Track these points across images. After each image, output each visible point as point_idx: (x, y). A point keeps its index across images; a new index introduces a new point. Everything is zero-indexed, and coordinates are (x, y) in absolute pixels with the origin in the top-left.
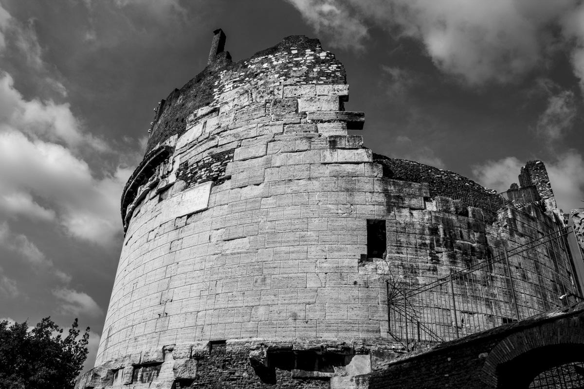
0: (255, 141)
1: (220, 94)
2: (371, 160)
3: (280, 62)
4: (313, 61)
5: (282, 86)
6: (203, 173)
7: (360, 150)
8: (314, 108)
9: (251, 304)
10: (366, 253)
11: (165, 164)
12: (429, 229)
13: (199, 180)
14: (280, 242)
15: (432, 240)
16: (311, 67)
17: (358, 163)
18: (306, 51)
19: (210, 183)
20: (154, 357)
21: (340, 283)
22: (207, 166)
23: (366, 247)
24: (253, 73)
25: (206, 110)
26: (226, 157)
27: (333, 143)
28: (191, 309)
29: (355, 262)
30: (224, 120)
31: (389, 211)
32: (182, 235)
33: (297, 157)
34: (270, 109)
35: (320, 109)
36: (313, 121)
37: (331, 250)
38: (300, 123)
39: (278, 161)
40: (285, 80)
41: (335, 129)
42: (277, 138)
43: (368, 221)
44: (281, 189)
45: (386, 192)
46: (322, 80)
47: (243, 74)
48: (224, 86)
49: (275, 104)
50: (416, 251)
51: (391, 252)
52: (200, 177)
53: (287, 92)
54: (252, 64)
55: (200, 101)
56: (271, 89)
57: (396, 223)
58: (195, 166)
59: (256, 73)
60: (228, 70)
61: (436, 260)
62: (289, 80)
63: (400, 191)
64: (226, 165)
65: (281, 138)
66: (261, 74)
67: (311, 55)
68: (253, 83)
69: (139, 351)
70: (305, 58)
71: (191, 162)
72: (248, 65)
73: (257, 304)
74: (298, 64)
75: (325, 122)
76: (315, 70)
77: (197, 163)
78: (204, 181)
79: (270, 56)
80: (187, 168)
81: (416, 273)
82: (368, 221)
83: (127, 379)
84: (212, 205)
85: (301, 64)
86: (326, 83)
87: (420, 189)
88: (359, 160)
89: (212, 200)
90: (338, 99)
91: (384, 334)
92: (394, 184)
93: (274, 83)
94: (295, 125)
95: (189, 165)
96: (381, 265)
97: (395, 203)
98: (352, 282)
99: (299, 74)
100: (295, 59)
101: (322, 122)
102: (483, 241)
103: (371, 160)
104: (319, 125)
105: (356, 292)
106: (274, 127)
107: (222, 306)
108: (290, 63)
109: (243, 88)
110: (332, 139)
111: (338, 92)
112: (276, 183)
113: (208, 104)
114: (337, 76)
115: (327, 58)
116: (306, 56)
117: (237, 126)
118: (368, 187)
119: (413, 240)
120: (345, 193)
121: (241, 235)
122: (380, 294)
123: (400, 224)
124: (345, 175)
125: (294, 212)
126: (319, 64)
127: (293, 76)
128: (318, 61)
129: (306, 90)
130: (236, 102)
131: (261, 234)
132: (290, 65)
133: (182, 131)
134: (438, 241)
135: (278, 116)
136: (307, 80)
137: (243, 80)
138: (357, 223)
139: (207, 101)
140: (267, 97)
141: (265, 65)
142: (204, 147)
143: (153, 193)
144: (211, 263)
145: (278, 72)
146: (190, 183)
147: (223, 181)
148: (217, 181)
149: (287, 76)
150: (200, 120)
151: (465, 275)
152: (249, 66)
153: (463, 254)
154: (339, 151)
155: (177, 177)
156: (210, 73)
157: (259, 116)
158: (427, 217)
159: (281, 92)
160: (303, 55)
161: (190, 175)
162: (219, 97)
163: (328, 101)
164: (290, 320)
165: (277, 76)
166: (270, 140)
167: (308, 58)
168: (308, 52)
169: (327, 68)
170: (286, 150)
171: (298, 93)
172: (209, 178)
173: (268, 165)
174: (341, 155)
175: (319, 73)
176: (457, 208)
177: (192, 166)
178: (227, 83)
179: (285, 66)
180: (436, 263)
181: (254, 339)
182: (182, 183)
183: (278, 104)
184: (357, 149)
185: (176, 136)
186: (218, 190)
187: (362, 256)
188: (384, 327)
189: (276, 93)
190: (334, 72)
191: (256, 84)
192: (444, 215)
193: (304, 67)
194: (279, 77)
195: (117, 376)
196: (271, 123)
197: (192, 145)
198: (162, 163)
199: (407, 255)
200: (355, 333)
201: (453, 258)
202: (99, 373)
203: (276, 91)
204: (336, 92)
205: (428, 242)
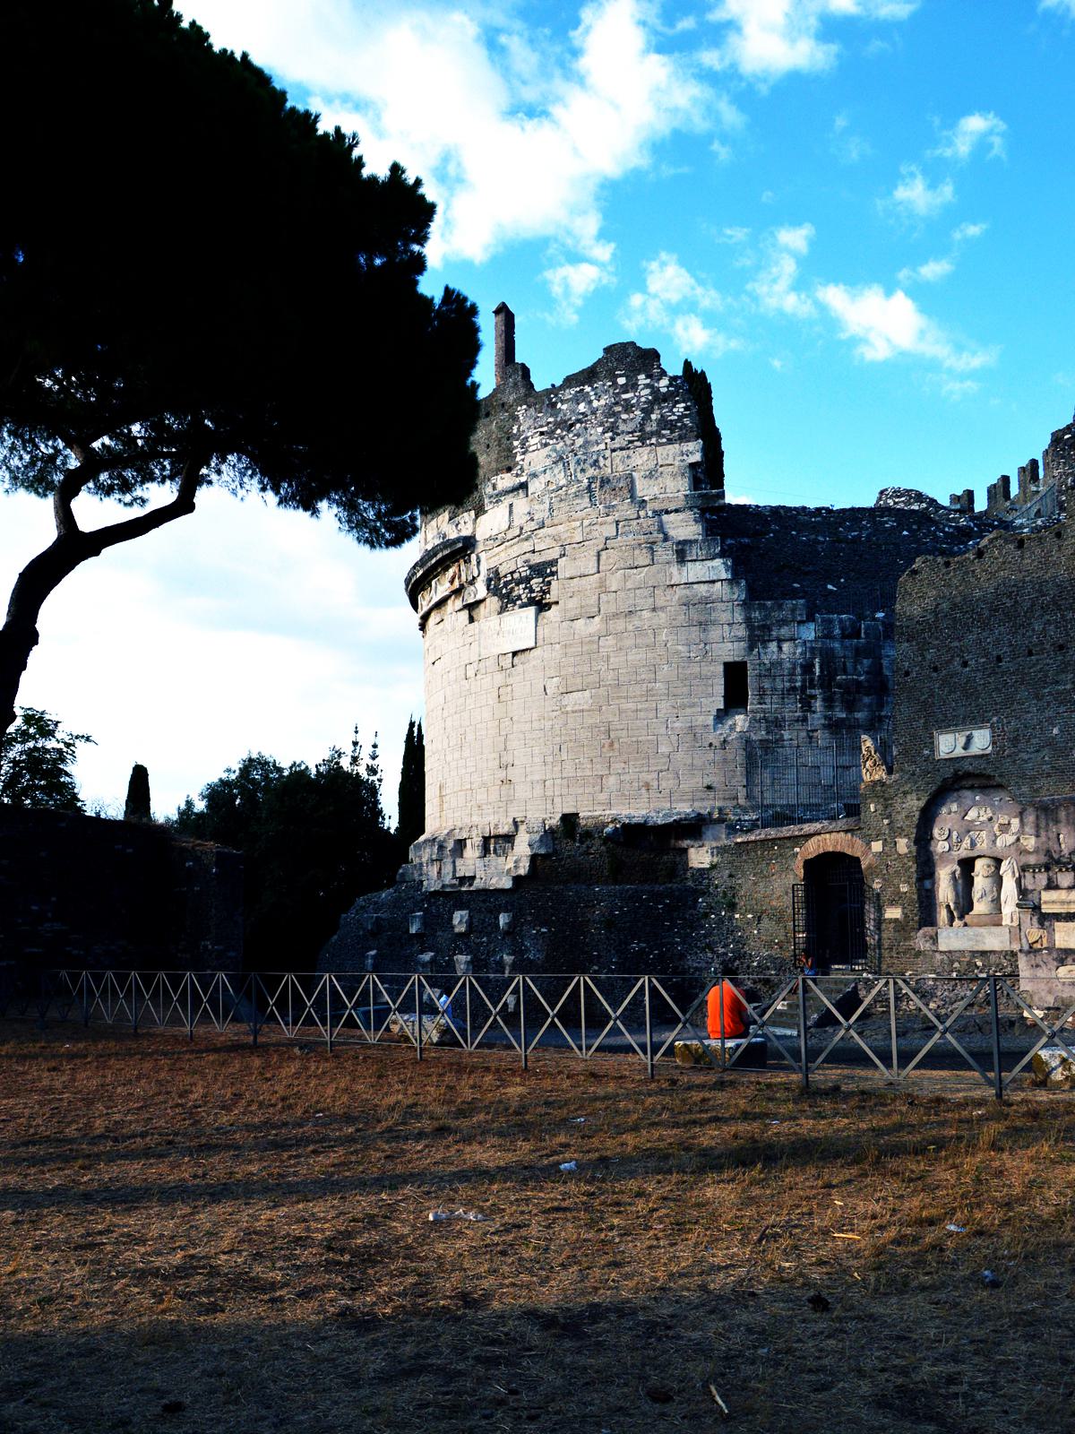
0: (582, 549)
1: (524, 453)
2: (730, 577)
3: (602, 402)
5: (609, 451)
6: (520, 590)
7: (717, 560)
8: (656, 488)
9: (601, 773)
10: (722, 707)
11: (465, 562)
12: (802, 666)
13: (519, 602)
14: (627, 697)
15: (804, 681)
16: (647, 412)
17: (713, 582)
18: (639, 377)
19: (532, 610)
20: (504, 830)
21: (694, 747)
22: (527, 580)
23: (722, 699)
24: (566, 422)
25: (505, 481)
26: (548, 571)
27: (682, 553)
28: (537, 777)
29: (710, 720)
30: (537, 507)
31: (751, 648)
32: (510, 681)
33: (639, 576)
34: (597, 494)
35: (663, 491)
36: (654, 512)
37: (683, 707)
38: (639, 517)
39: (614, 582)
40: (612, 439)
41: (685, 527)
43: (726, 665)
44: (620, 625)
45: (748, 621)
46: (664, 436)
47: (551, 420)
48: (527, 438)
49: (601, 487)
50: (783, 698)
51: (752, 704)
52: (519, 597)
53: (617, 461)
54: (563, 402)
55: (497, 460)
56: (595, 457)
57: (760, 665)
58: (509, 578)
60: (529, 406)
61: (807, 704)
62: (618, 439)
63: (766, 617)
66: (578, 425)
67: (647, 386)
68: (569, 442)
69: (486, 820)
71: (503, 571)
72: (556, 403)
73: (607, 772)
74: (628, 407)
75: (671, 512)
76: (653, 417)
77: (512, 573)
79: (587, 389)
80: (500, 579)
81: (781, 726)
83: (477, 853)
84: (540, 642)
85: (633, 406)
86: (670, 442)
87: (793, 610)
88: (715, 578)
89: (540, 637)
90: (688, 470)
91: (742, 801)
92: (762, 607)
93: (598, 444)
94: (631, 522)
95: (501, 575)
96: (740, 721)
97: (758, 636)
98: (706, 744)
100: (624, 396)
101: (667, 512)
102: (876, 670)
103: (730, 577)
104: (665, 518)
105: (711, 756)
106: (604, 527)
107: (570, 775)
108: (616, 404)
109: (555, 450)
110: (680, 547)
112: (616, 615)
113: (509, 470)
114: (686, 425)
116: (640, 387)
117: (556, 521)
118: (725, 617)
119: (780, 686)
121: (580, 688)
122: (737, 755)
123: (765, 664)
125: (638, 657)
126: (659, 404)
127: (623, 432)
128: (658, 398)
129: (642, 458)
130: (548, 476)
131: (604, 686)
132: (618, 409)
133: (480, 511)
134: (812, 680)
135: (608, 507)
136: (642, 439)
137: (553, 432)
138: (712, 669)
139: (507, 463)
140: (591, 472)
141: (582, 407)
142: (516, 550)
143: (459, 604)
144: (550, 723)
145: (601, 424)
146: (507, 603)
147: (548, 606)
148: (542, 606)
149: (613, 429)
150: (502, 498)
151: (843, 719)
152: (559, 405)
153: (842, 694)
154: (689, 564)
155: (488, 589)
156: (503, 405)
157: (582, 507)
158: (799, 650)
159: (608, 463)
161: (504, 591)
162: (523, 460)
163: (674, 475)
164: (643, 791)
165: (600, 430)
166: (601, 546)
167: (642, 393)
168: (642, 377)
169: (671, 411)
170: (622, 566)
172: (531, 602)
173: (603, 588)
174: (695, 571)
176: (842, 629)
177: (505, 576)
178: (529, 434)
179: (610, 412)
180: (807, 711)
181: (607, 812)
182: (493, 603)
183: (607, 487)
185: (473, 513)
186: (545, 621)
187: (718, 710)
188: (742, 793)
189: (601, 465)
190: (681, 418)
191: (573, 444)
192: (823, 643)
193: (638, 413)
194: (604, 433)
195: (465, 846)
196: (600, 520)
197: (498, 540)
198: (462, 561)
200: (711, 802)
201: (829, 702)
202: (445, 844)
203: (601, 459)
204: (685, 457)
205: (798, 684)
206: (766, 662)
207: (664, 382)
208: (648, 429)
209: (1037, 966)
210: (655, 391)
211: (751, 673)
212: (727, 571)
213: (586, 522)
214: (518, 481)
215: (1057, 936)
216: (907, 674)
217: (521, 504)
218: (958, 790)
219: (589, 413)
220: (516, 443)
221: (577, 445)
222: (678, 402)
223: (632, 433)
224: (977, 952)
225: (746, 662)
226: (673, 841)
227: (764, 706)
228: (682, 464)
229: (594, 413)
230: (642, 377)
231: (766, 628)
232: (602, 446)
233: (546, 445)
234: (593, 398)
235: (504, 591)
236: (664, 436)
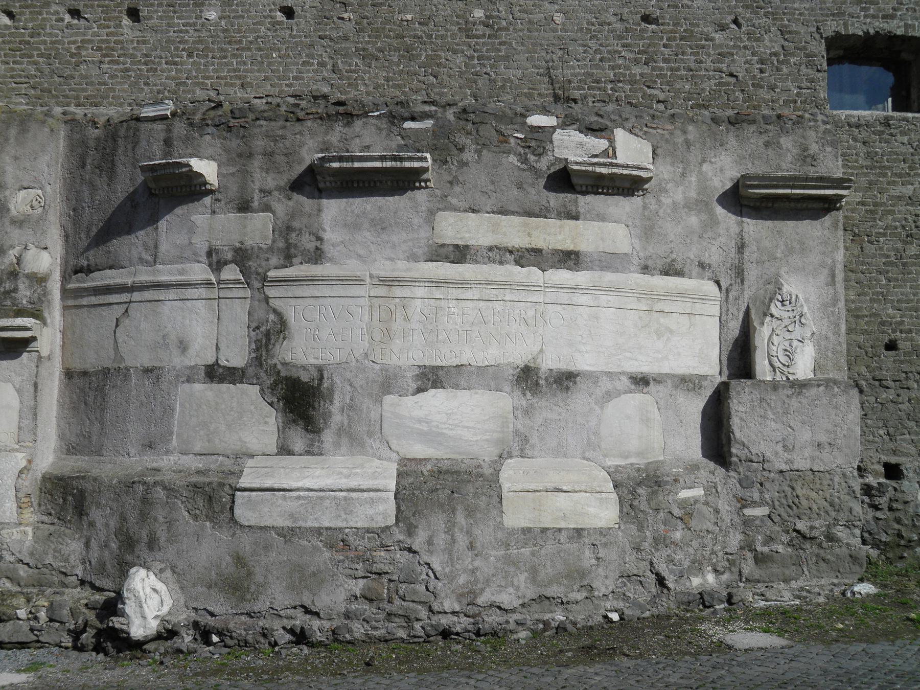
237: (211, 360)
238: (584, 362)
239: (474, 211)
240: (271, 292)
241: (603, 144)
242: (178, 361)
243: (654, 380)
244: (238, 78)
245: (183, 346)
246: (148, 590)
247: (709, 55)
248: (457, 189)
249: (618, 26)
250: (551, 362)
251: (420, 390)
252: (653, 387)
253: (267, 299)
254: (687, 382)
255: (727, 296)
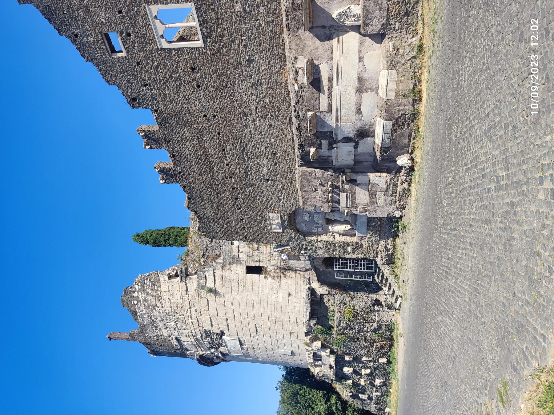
3: (144, 309)
4: (142, 292)
9: (289, 323)
17: (214, 276)
18: (134, 296)
26: (209, 333)
31: (241, 264)
36: (186, 294)
40: (158, 307)
42: (198, 311)
43: (247, 273)
47: (150, 327)
50: (261, 253)
59: (151, 321)
64: (213, 333)
65: (199, 310)
66: (153, 318)
70: (141, 297)
74: (146, 300)
76: (150, 292)
77: (210, 343)
78: (222, 341)
79: (138, 314)
82: (247, 273)
88: (213, 275)
93: (160, 312)
99: (153, 300)
100: (142, 302)
101: (187, 290)
108: (144, 305)
110: (200, 287)
111: (165, 281)
115: (139, 284)
116: (138, 296)
120: (232, 283)
123: (248, 259)
124: (222, 283)
127: (155, 303)
128: (143, 290)
129: (165, 296)
132: (146, 304)
149: (154, 307)
152: (145, 323)
159: (167, 309)
160: (138, 297)
161: (217, 346)
162: (166, 336)
165: (154, 311)
168: (135, 295)
171: (167, 300)
172: (221, 338)
175: (152, 290)
182: (221, 349)
184: (206, 276)
189: (168, 312)
199: (263, 257)
203: (166, 312)
204: (166, 281)
206: (246, 258)
207: (136, 287)
208: (154, 294)
209: (376, 211)
210: (140, 290)
211: (250, 264)
212: (210, 271)
213: (190, 319)
214: (174, 339)
215: (362, 202)
216: (246, 238)
217: (184, 339)
218: (296, 224)
219: (148, 314)
220: (160, 338)
221: (160, 319)
222: (144, 283)
223: (156, 301)
224: (368, 226)
225: (247, 267)
226: (317, 299)
227: (264, 261)
228: (169, 282)
229: (148, 312)
230: (134, 295)
231: (233, 258)
232: (161, 310)
233: (160, 329)
234: (142, 312)
235: (217, 346)
236: (157, 288)
237: (353, 148)
238: (356, 76)
239: (320, 103)
240: (339, 139)
241: (300, 71)
242: (353, 152)
243: (360, 54)
244: (287, 135)
245: (350, 152)
246: (402, 162)
247: (268, 28)
248: (315, 107)
249: (264, 53)
250: (355, 84)
251: (361, 113)
252: (362, 55)
253: (340, 140)
254: (361, 44)
255: (337, 30)
